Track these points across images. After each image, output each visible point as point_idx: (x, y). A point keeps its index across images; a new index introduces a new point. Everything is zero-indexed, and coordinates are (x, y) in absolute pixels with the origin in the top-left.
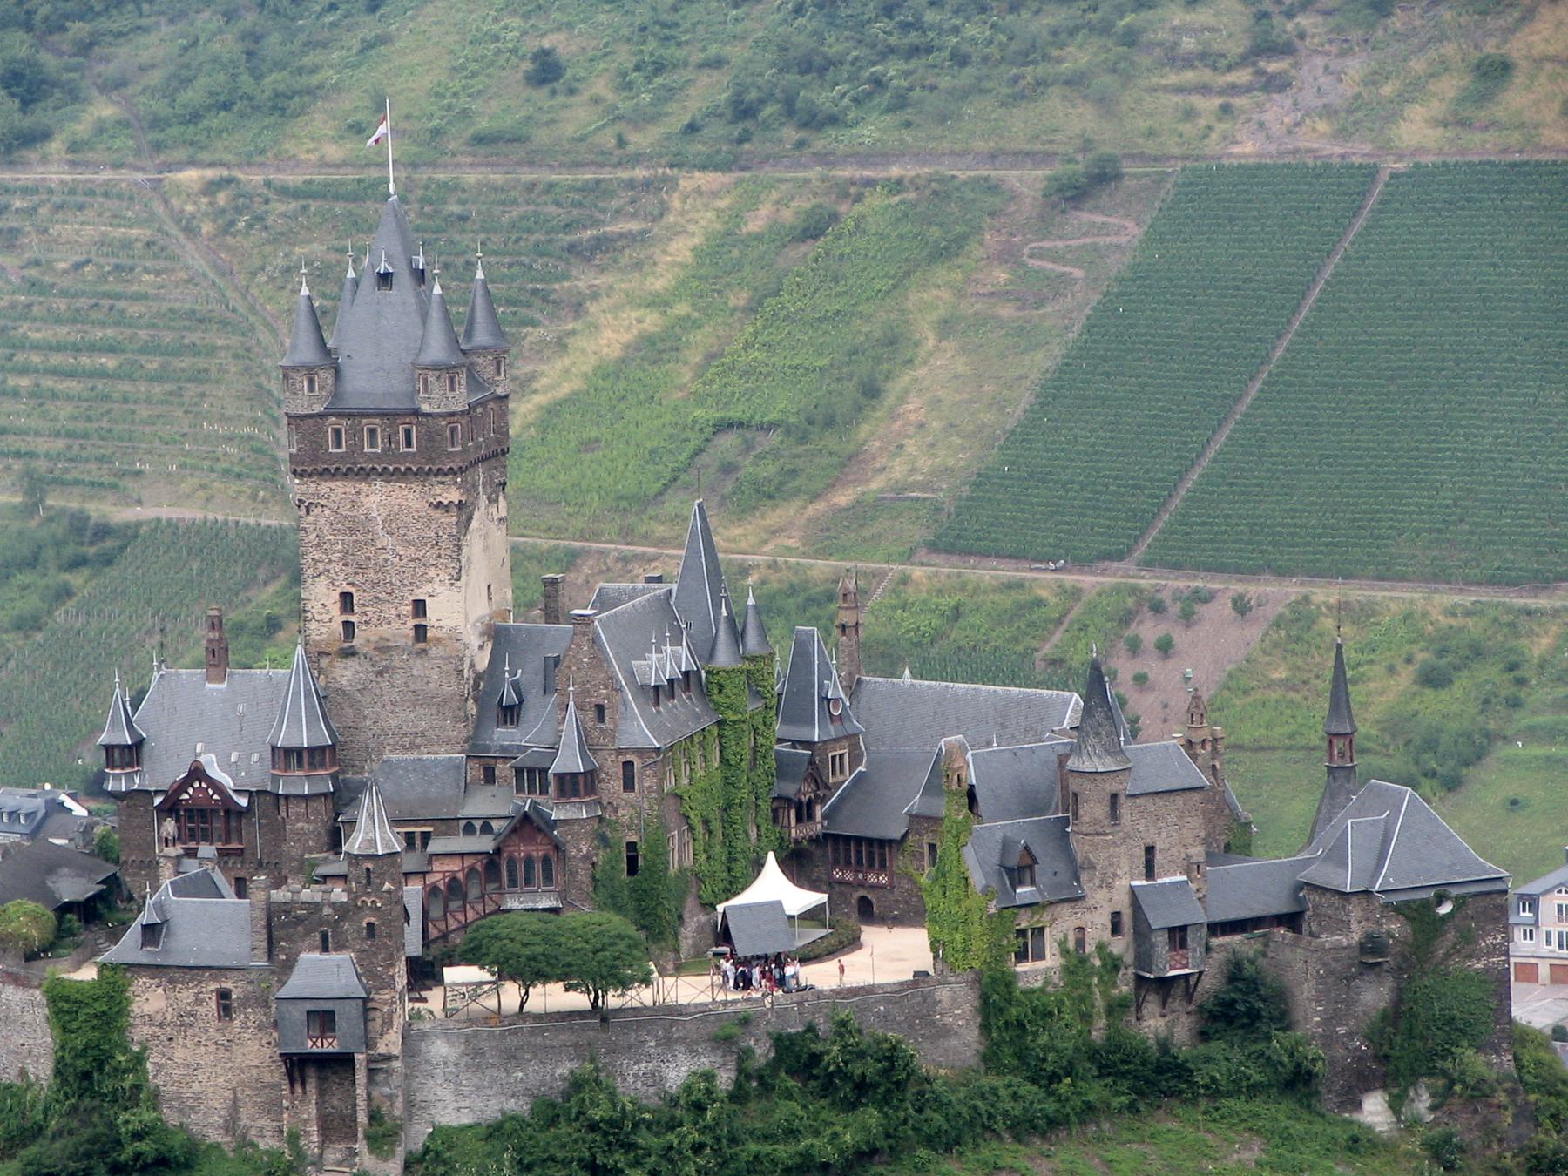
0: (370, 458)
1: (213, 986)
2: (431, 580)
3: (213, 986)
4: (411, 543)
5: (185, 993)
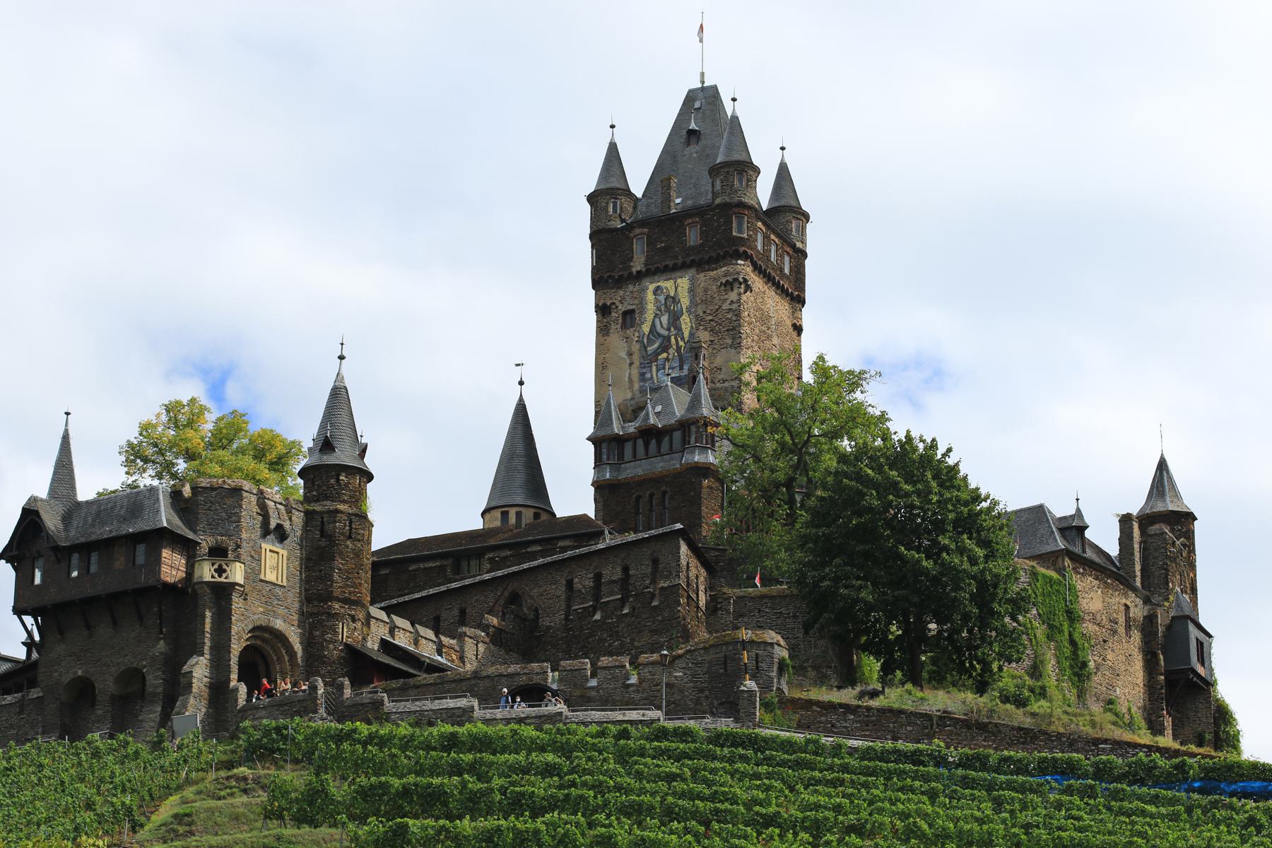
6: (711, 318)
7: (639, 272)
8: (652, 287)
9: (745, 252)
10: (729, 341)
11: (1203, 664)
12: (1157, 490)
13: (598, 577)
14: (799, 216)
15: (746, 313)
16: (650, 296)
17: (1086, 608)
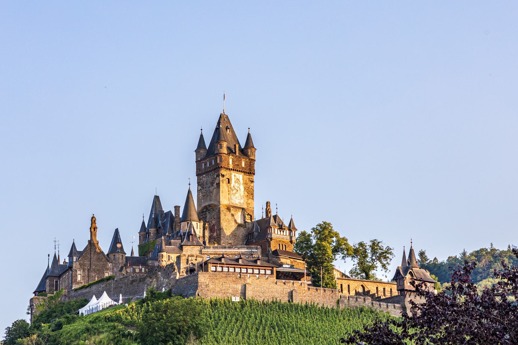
6: (247, 189)
7: (231, 169)
8: (233, 174)
10: (252, 197)
13: (384, 289)
16: (233, 176)
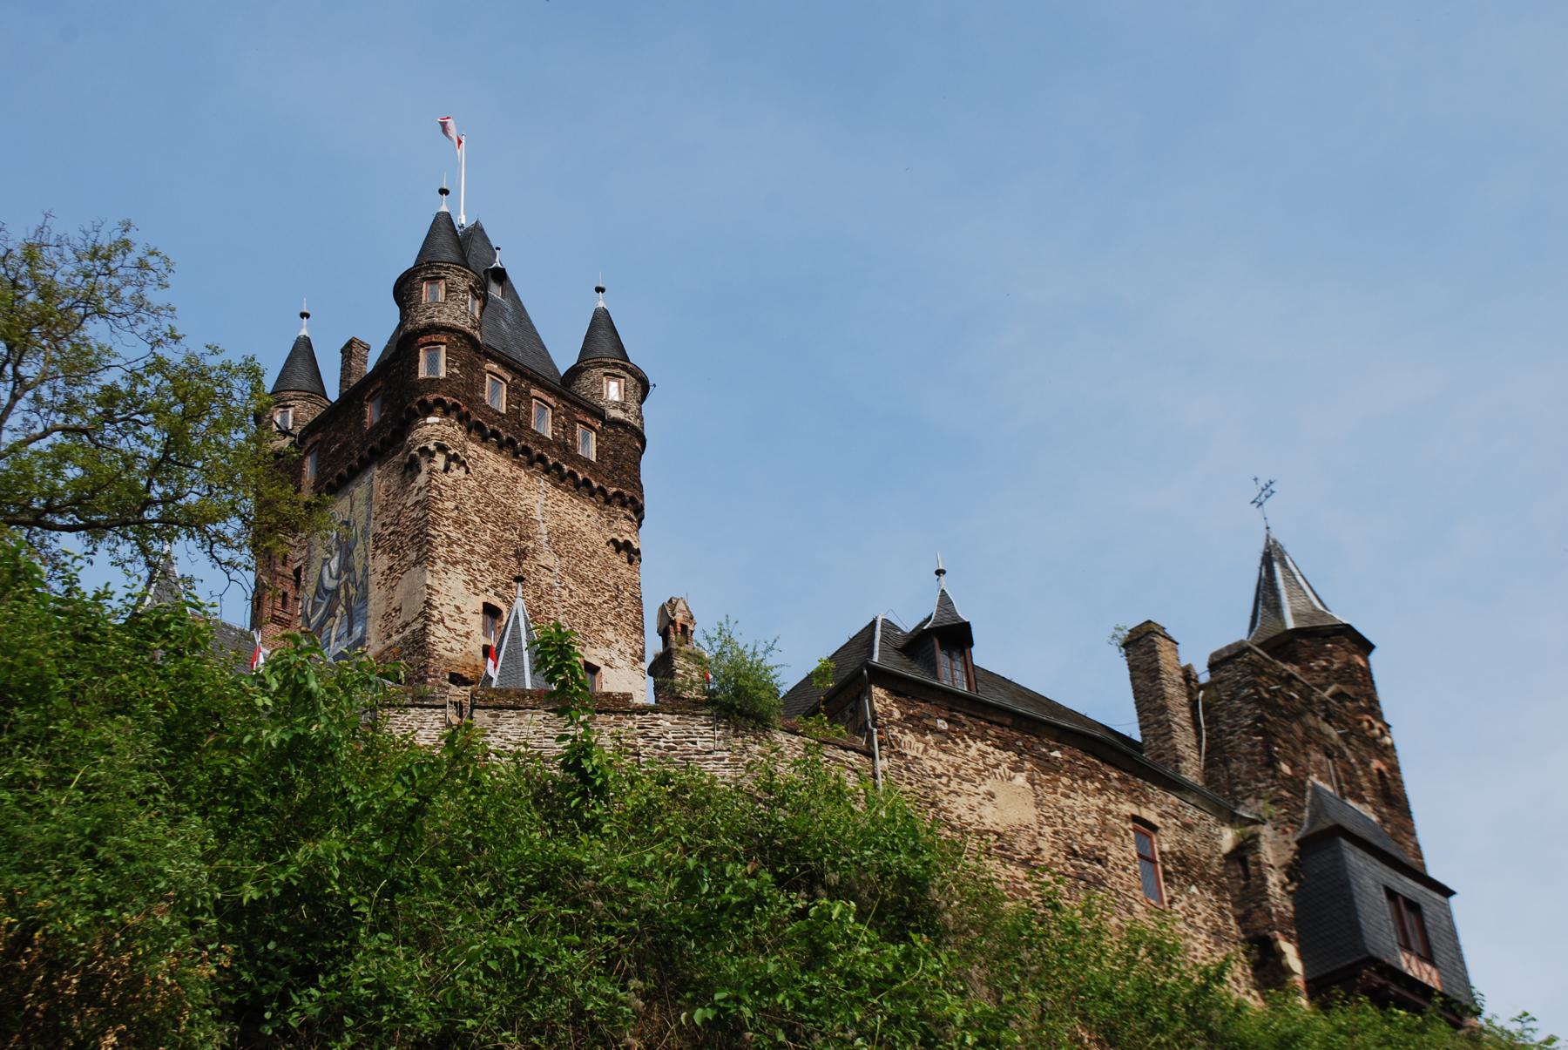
0: (540, 439)
1: (1128, 808)
2: (609, 644)
3: (1128, 808)
4: (583, 580)
5: (1078, 801)
9: (439, 402)
11: (1428, 957)
12: (1265, 604)
14: (616, 371)
15: (450, 505)
17: (967, 818)
